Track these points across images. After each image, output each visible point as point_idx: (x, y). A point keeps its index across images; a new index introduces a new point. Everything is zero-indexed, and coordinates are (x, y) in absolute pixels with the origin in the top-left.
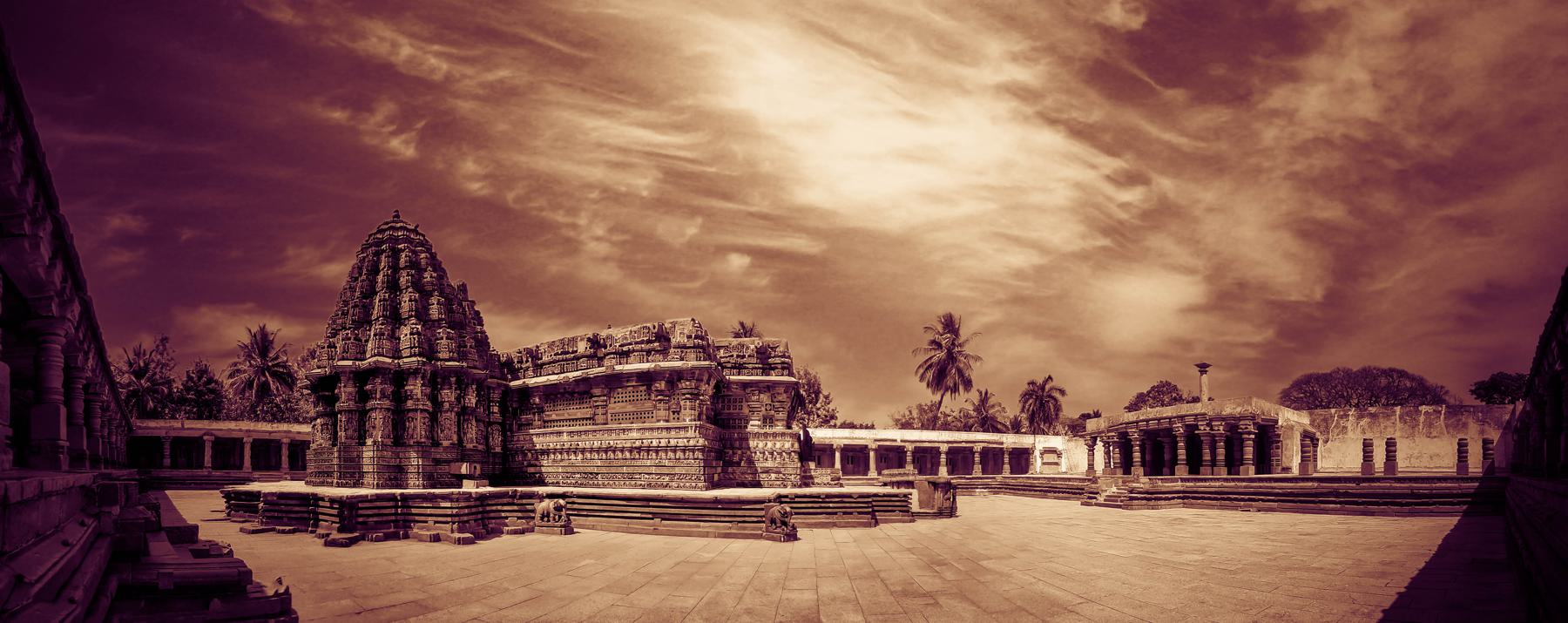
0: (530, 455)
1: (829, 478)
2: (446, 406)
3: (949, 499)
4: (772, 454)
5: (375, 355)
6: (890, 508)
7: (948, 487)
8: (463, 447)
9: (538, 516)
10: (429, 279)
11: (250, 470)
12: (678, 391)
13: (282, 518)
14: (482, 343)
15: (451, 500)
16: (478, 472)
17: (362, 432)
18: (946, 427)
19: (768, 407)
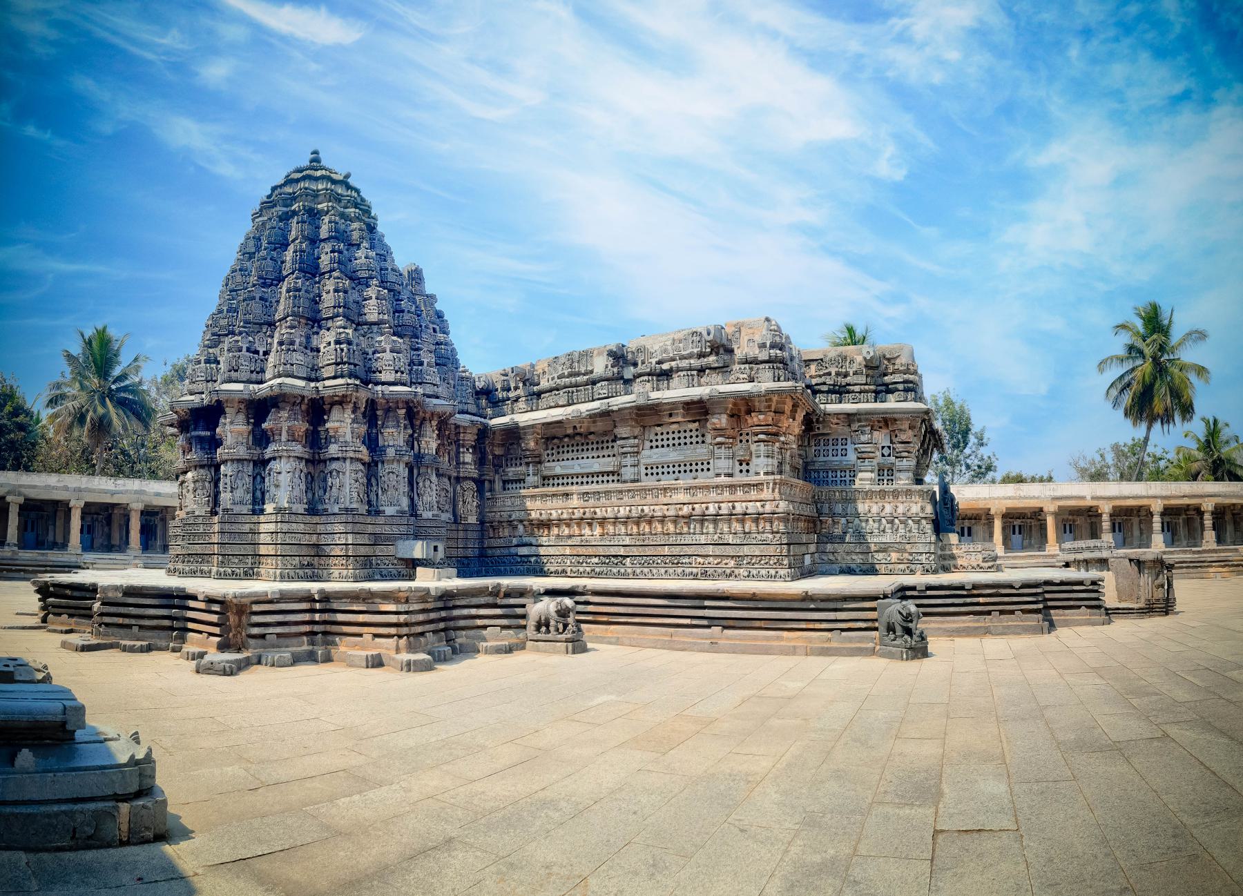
0: (521, 527)
1: (980, 557)
2: (391, 452)
3: (1162, 586)
4: (892, 522)
5: (280, 376)
6: (1072, 603)
7: (1161, 566)
8: (416, 516)
9: (531, 623)
10: (363, 260)
11: (79, 551)
12: (748, 430)
13: (129, 626)
14: (446, 360)
15: (397, 601)
16: (441, 554)
17: (258, 494)
18: (1158, 476)
19: (886, 452)
